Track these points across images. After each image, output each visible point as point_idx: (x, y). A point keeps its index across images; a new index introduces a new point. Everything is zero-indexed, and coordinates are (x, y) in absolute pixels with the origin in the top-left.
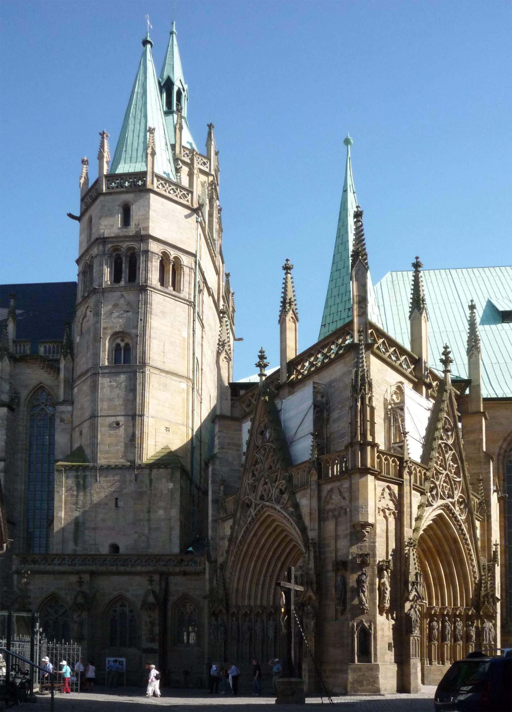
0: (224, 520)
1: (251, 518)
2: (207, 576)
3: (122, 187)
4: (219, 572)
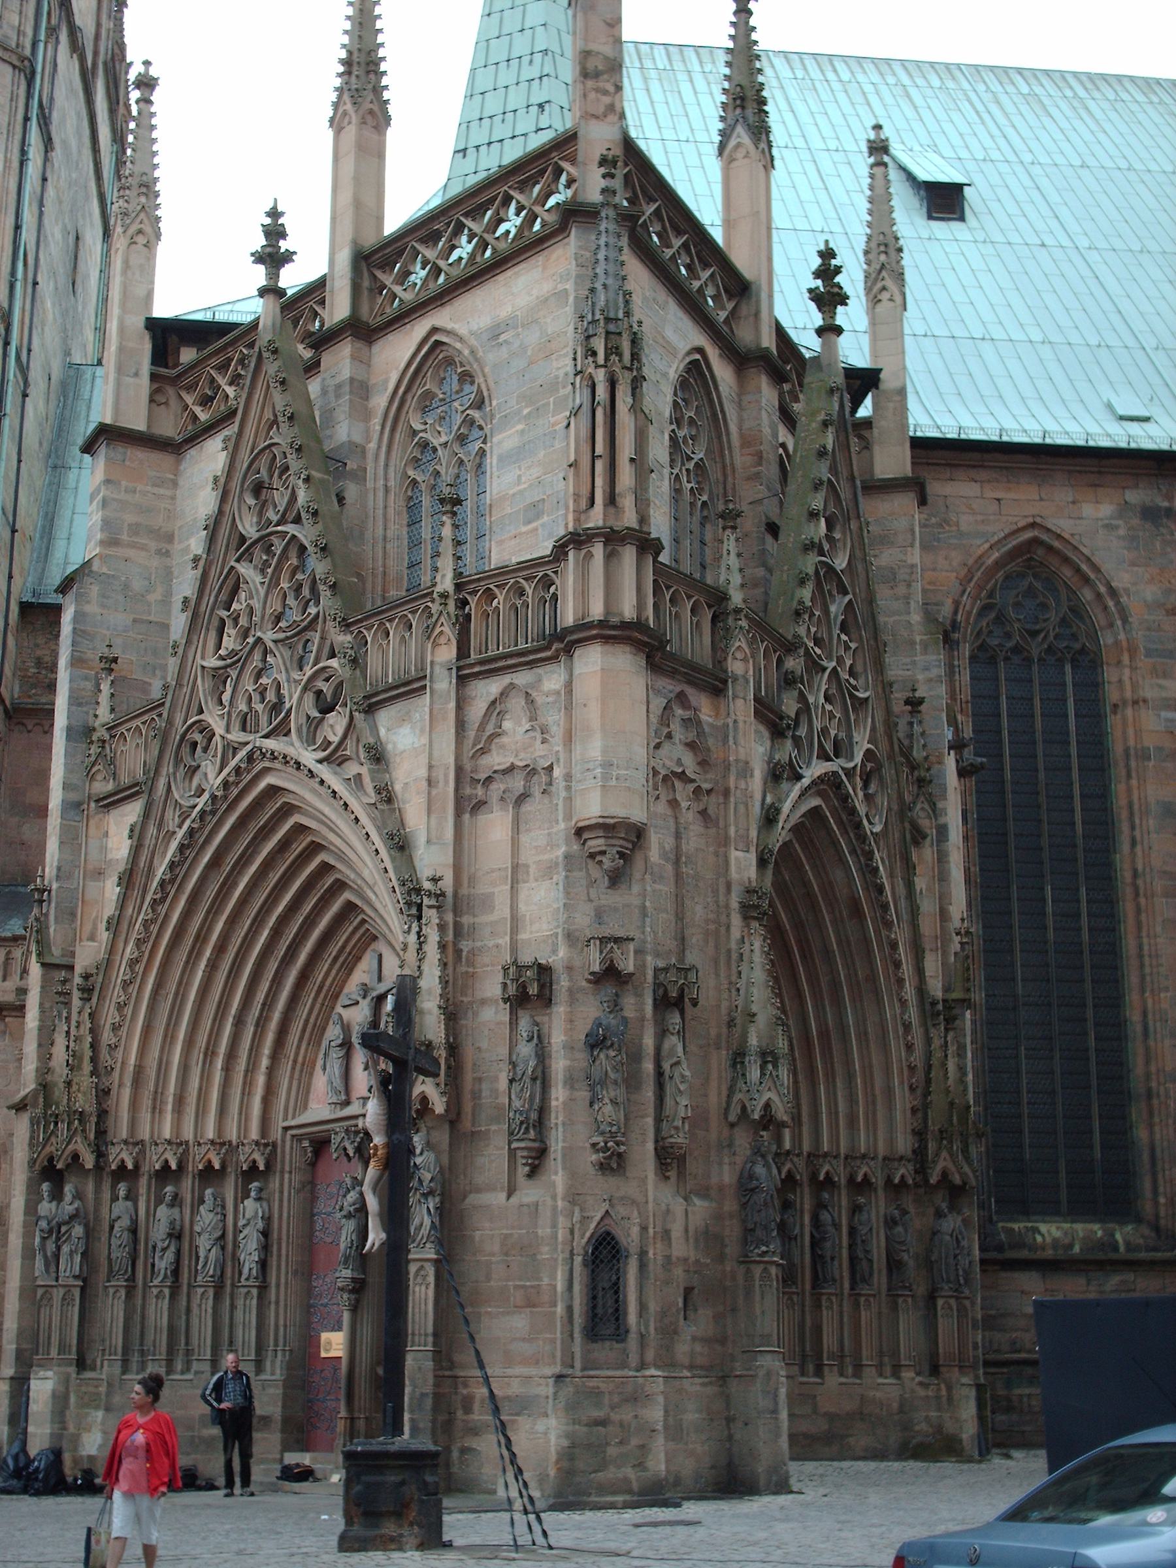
0: (109, 802)
1: (206, 796)
4: (76, 1002)
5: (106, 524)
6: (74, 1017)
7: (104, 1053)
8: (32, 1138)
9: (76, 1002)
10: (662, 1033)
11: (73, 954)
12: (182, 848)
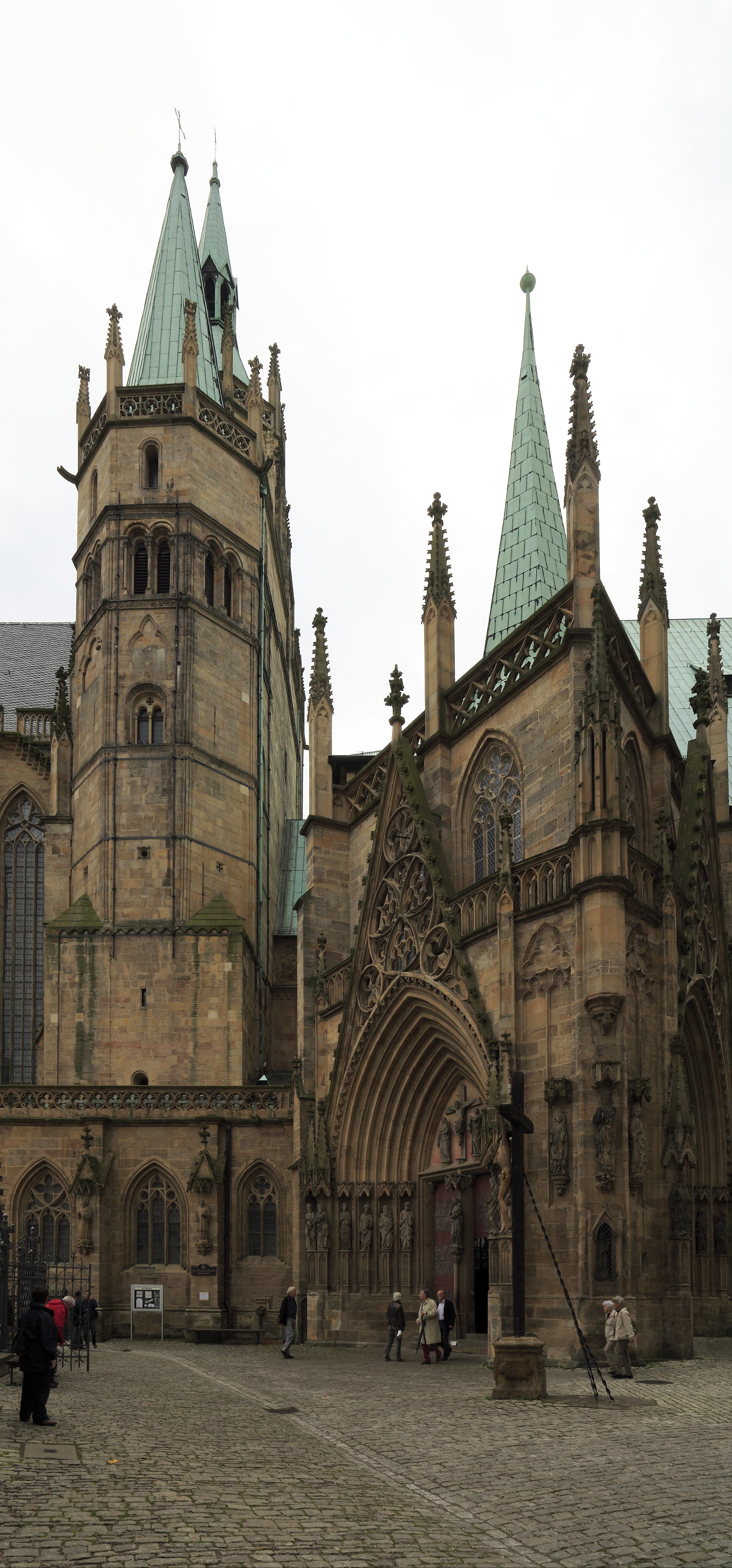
0: (327, 1015)
3: (144, 413)
4: (317, 1116)
5: (316, 871)
6: (317, 1123)
7: (332, 1141)
8: (301, 1183)
9: (317, 1116)
10: (631, 1117)
11: (314, 1093)
12: (365, 1034)
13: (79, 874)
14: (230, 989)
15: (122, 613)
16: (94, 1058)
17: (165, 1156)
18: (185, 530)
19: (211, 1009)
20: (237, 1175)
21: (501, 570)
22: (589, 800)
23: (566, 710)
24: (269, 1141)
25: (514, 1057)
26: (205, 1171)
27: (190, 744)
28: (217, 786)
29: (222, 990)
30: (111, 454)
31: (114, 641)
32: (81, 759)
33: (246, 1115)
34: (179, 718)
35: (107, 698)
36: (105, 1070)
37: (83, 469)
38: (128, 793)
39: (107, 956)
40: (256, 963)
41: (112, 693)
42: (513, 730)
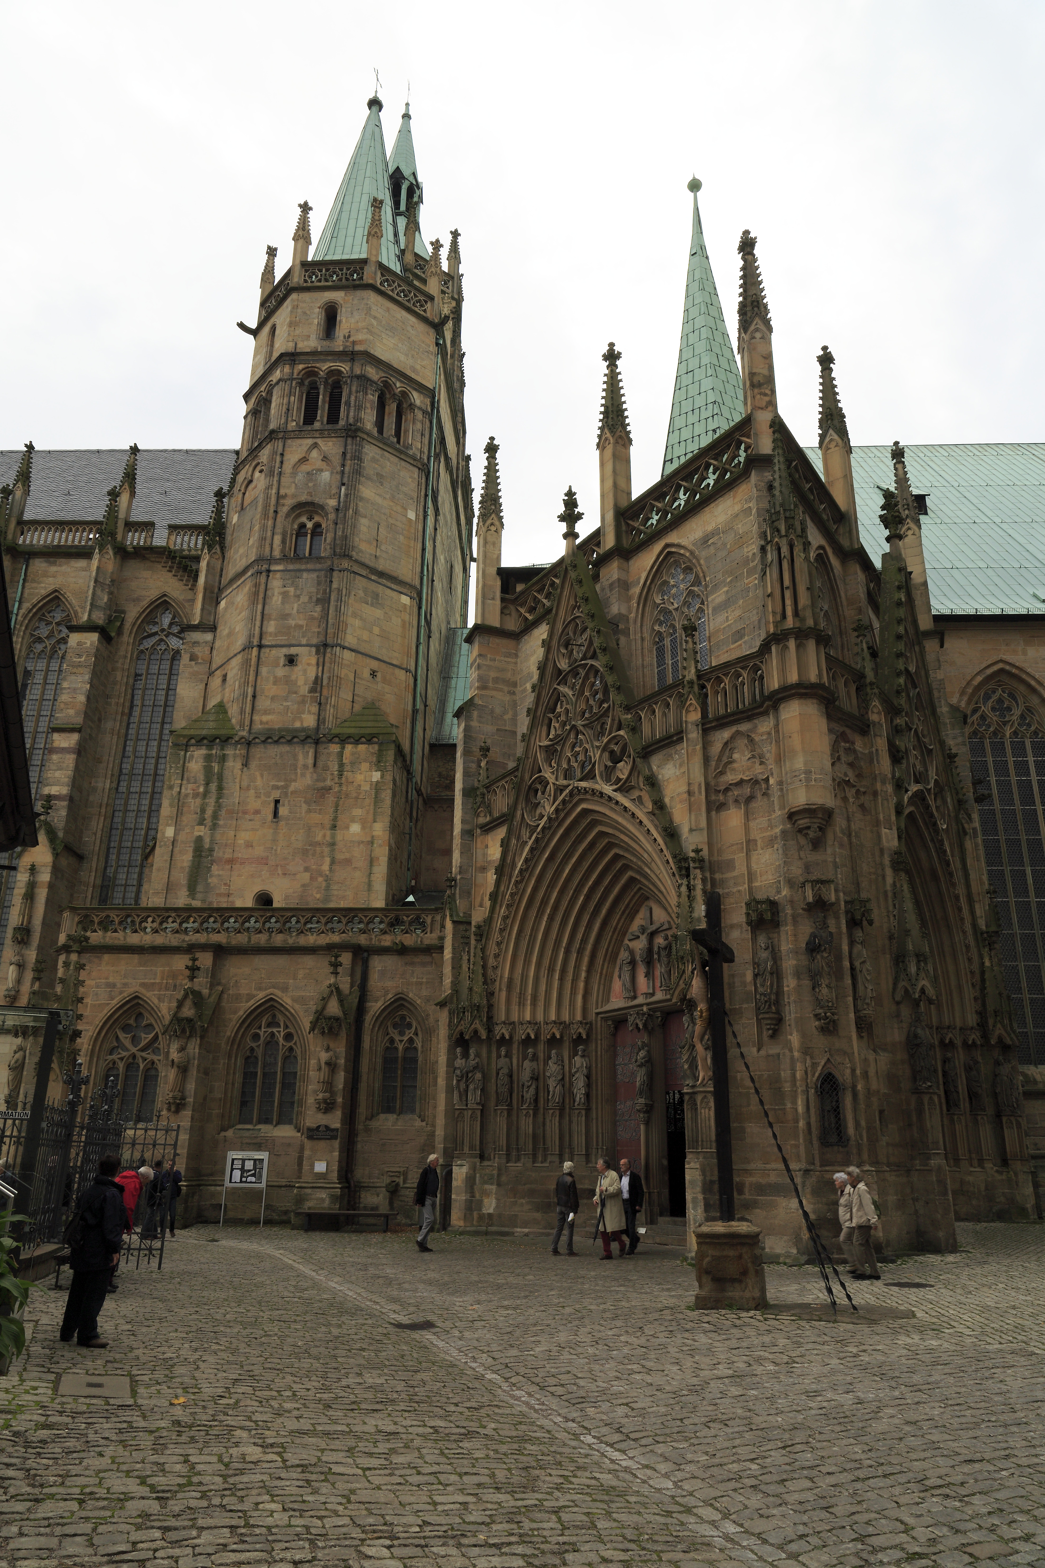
0: (487, 829)
2: (448, 954)
3: (326, 280)
4: (473, 942)
6: (472, 951)
7: (490, 972)
8: (450, 1022)
9: (473, 942)
10: (852, 943)
11: (470, 916)
12: (532, 849)
13: (216, 681)
14: (377, 800)
15: (289, 441)
16: (211, 876)
17: (285, 989)
18: (358, 372)
19: (353, 821)
20: (372, 1013)
21: (677, 405)
22: (779, 609)
23: (750, 526)
24: (413, 972)
25: (708, 875)
26: (334, 1008)
27: (350, 557)
28: (376, 596)
29: (367, 801)
30: (291, 312)
31: (278, 465)
32: (231, 571)
33: (387, 941)
34: (339, 533)
35: (265, 515)
36: (223, 889)
37: (261, 324)
38: (279, 602)
39: (238, 765)
40: (409, 772)
41: (272, 511)
42: (694, 544)
